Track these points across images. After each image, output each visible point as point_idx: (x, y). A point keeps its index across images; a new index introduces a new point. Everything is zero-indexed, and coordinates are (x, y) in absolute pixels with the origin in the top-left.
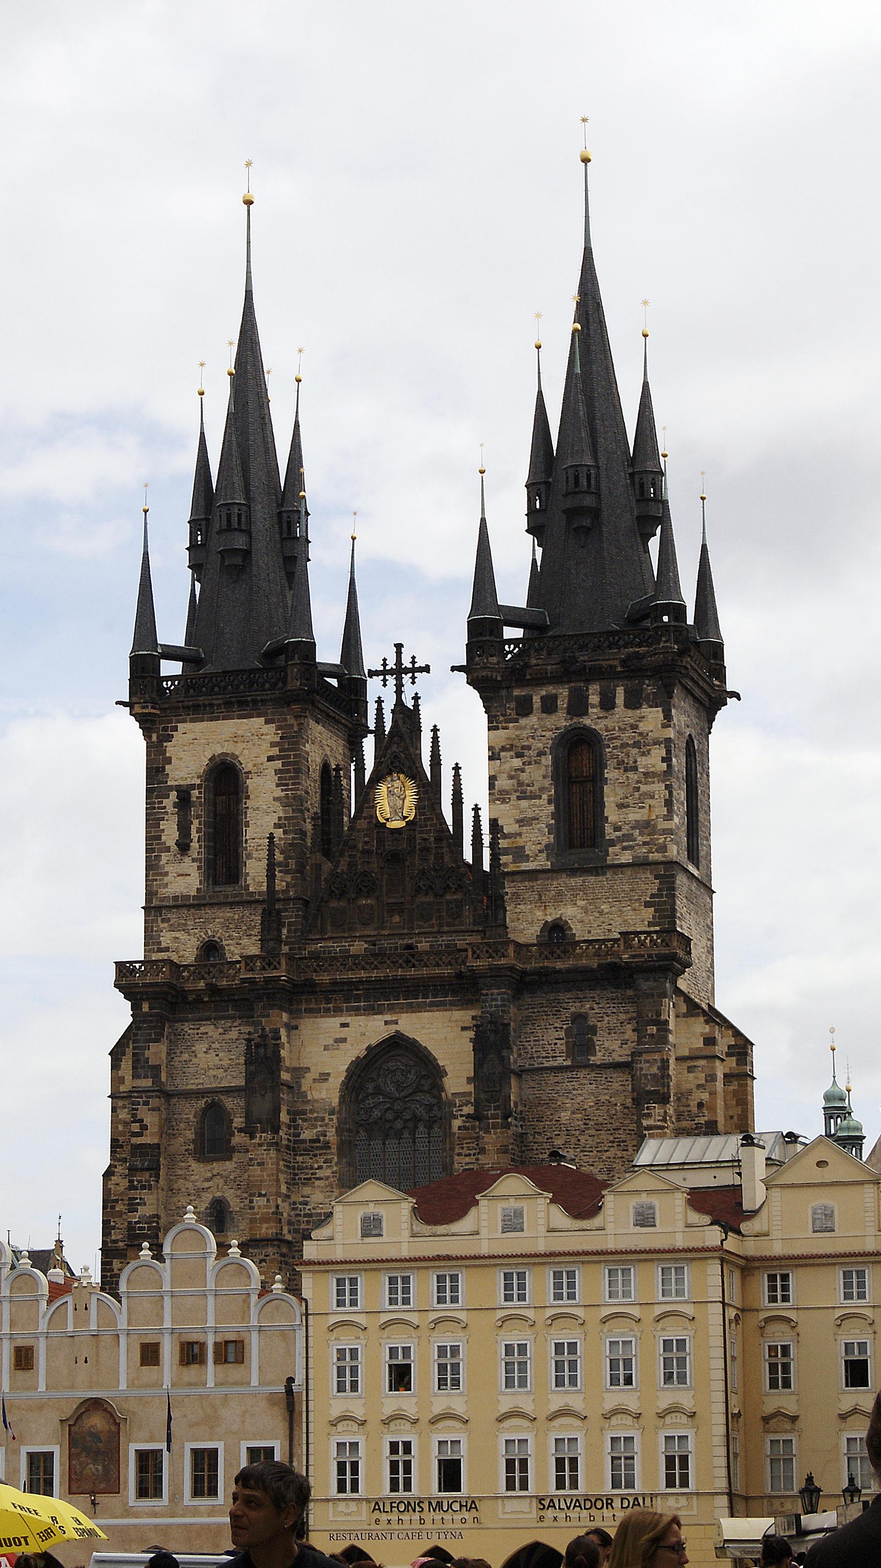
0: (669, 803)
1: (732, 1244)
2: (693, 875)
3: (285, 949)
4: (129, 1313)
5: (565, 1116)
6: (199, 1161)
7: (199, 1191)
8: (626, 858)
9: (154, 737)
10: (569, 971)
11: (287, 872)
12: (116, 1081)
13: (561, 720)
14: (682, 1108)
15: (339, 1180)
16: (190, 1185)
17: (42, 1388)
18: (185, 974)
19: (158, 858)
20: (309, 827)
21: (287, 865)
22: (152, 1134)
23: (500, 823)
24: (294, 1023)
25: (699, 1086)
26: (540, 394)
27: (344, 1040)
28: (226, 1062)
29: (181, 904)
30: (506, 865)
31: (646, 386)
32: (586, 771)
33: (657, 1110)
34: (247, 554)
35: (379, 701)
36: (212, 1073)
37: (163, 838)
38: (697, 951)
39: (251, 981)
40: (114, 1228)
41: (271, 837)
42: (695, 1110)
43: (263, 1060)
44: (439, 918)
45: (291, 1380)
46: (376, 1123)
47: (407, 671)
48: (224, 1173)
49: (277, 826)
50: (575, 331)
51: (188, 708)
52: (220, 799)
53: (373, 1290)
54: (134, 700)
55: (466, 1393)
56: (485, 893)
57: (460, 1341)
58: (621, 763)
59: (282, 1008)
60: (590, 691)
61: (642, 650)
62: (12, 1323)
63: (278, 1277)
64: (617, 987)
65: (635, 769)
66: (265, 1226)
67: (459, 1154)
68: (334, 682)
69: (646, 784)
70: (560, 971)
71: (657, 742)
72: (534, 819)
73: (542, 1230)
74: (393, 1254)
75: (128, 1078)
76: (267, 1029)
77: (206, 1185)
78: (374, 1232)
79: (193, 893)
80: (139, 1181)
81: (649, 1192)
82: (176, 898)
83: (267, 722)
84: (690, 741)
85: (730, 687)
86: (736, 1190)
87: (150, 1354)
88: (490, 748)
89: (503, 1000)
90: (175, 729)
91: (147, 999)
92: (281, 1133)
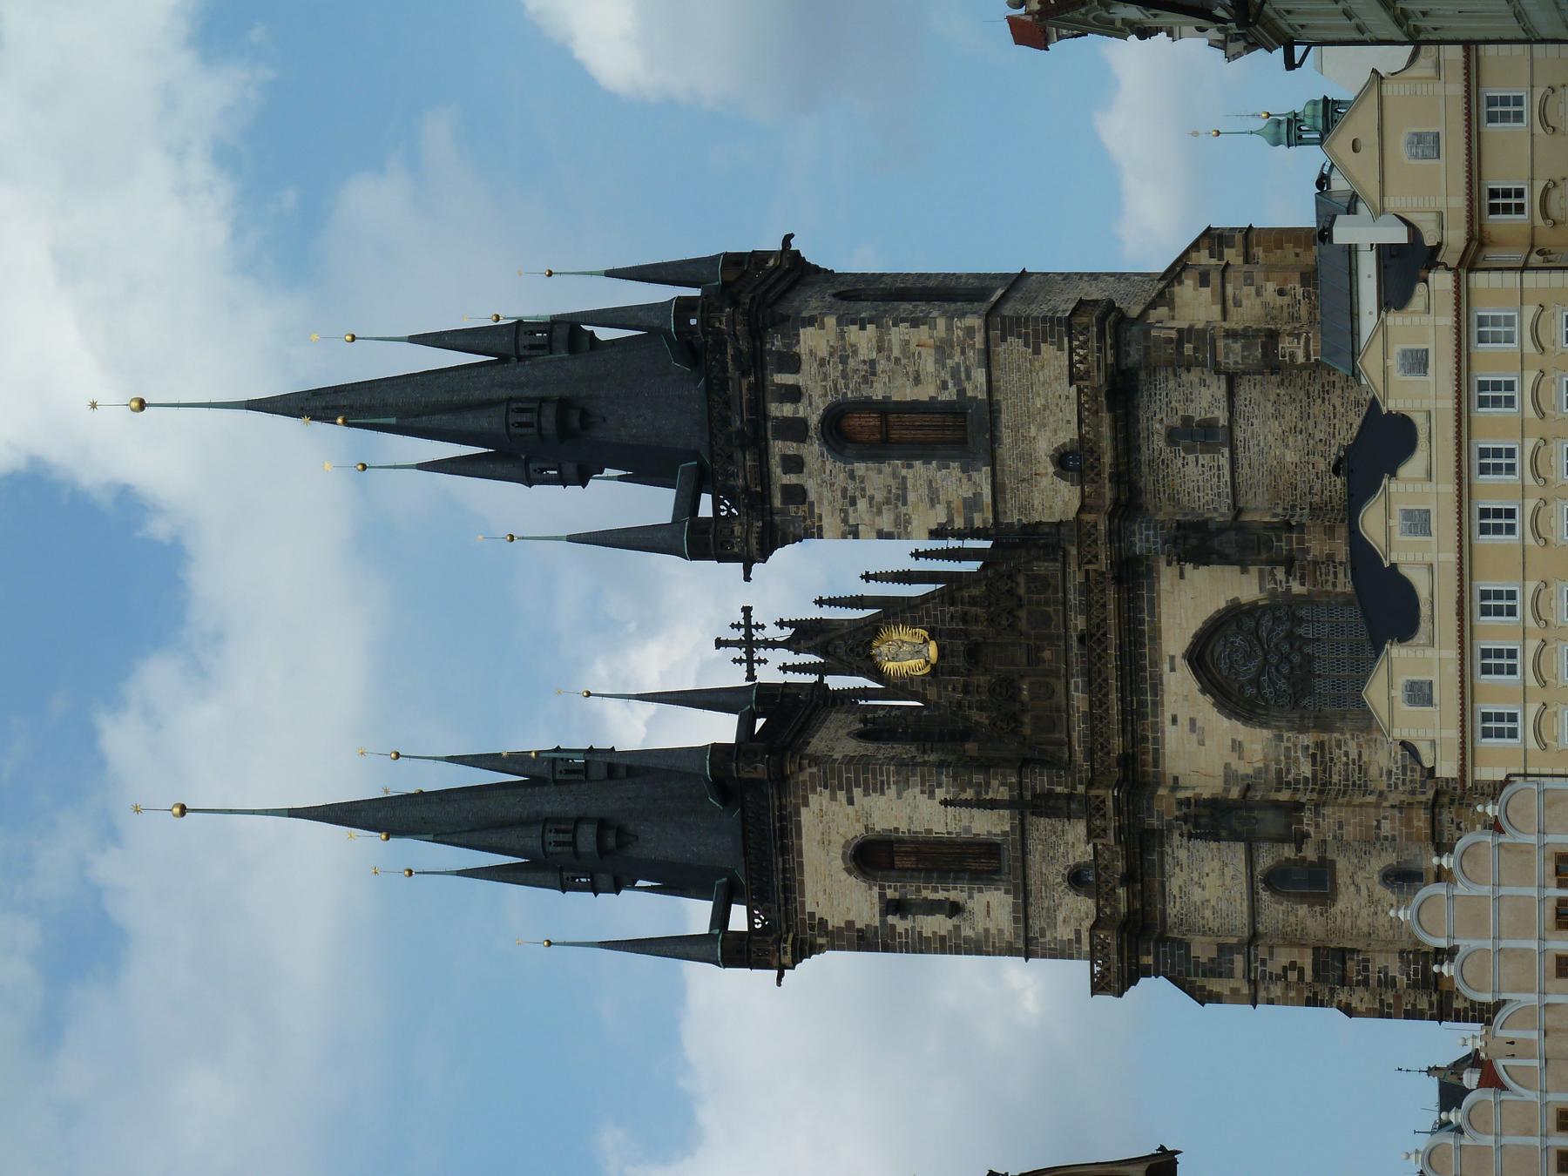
0: (915, 323)
1: (1450, 256)
2: (1003, 296)
3: (1081, 789)
5: (1290, 457)
6: (1334, 901)
7: (1372, 901)
8: (980, 375)
9: (821, 941)
10: (1115, 448)
11: (988, 785)
12: (1235, 997)
13: (812, 451)
14: (1285, 315)
16: (1364, 912)
18: (1108, 911)
19: (967, 940)
20: (933, 757)
21: (979, 785)
23: (934, 527)
24: (1170, 782)
25: (1258, 294)
26: (423, 467)
27: (1193, 722)
28: (1216, 864)
29: (1023, 914)
30: (984, 521)
31: (414, 339)
32: (873, 421)
33: (1286, 344)
34: (603, 825)
35: (785, 668)
36: (1228, 881)
37: (943, 933)
38: (1094, 293)
39: (1119, 830)
40: (1414, 1006)
41: (945, 803)
42: (1287, 300)
43: (1215, 818)
44: (1047, 603)
47: (749, 635)
48: (1351, 869)
49: (932, 795)
50: (346, 423)
51: (786, 899)
52: (898, 862)
54: (775, 962)
56: (1018, 545)
58: (865, 380)
59: (1154, 792)
61: (730, 351)
63: (1479, 808)
64: (1135, 390)
65: (873, 363)
66: (1416, 823)
67: (1334, 585)
68: (760, 722)
69: (891, 350)
70: (1116, 458)
71: (842, 336)
73: (1428, 487)
74: (1453, 669)
75: (1233, 983)
77: (1364, 892)
79: (1010, 899)
80: (1359, 973)
82: (1016, 920)
83: (806, 804)
84: (842, 296)
85: (778, 247)
86: (1385, 253)
88: (844, 536)
89: (1148, 529)
90: (812, 915)
92: (1303, 800)
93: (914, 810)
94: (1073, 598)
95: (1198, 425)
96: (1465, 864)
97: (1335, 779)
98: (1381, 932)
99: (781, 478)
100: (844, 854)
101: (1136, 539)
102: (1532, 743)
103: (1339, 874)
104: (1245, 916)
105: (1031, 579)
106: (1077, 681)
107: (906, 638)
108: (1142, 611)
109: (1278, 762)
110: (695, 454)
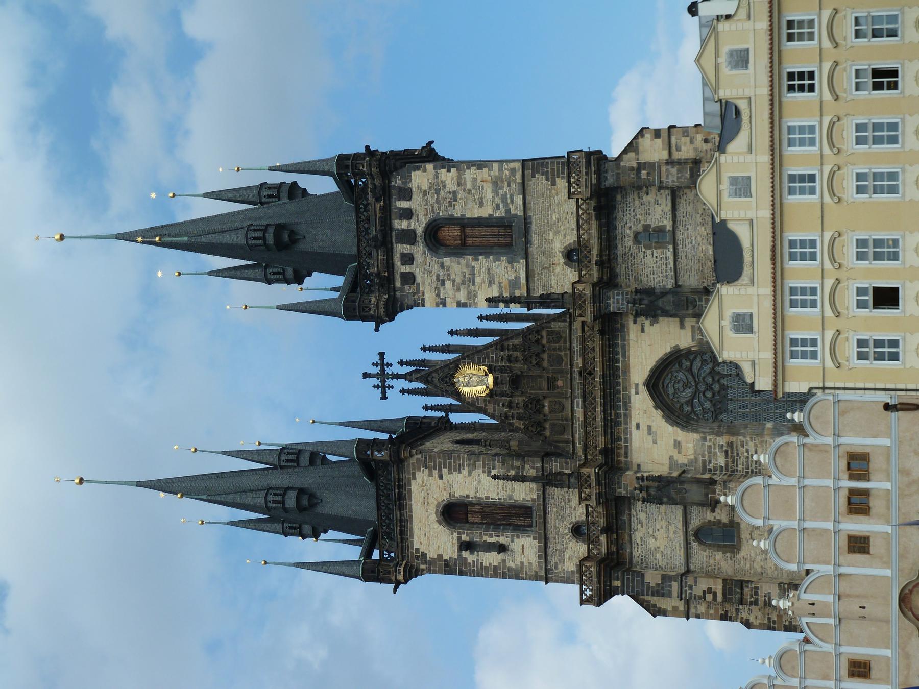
4: (819, 563)
6: (739, 550)
8: (519, 200)
9: (423, 567)
11: (523, 467)
12: (675, 613)
13: (419, 250)
15: (757, 435)
16: (759, 558)
17: (888, 653)
19: (510, 569)
22: (715, 585)
24: (635, 468)
25: (692, 142)
27: (649, 427)
28: (664, 523)
29: (544, 554)
32: (455, 231)
34: (301, 491)
36: (671, 535)
39: (599, 496)
40: (790, 622)
42: (709, 145)
43: (662, 489)
44: (560, 349)
45: (887, 407)
46: (714, 405)
53: (802, 323)
54: (393, 578)
55: (902, 233)
57: (852, 238)
58: (450, 204)
60: (399, 227)
62: (826, 677)
63: (789, 415)
64: (614, 208)
65: (455, 193)
70: (601, 251)
71: (436, 176)
72: (489, 273)
73: (750, 158)
74: (768, 304)
76: (637, 486)
78: (748, 321)
79: (536, 543)
80: (751, 596)
81: (717, 55)
82: (540, 557)
83: (415, 479)
87: (859, 545)
88: (437, 305)
89: (618, 294)
90: (417, 550)
91: (610, 582)
93: (477, 483)
94: (576, 346)
95: (654, 230)
96: (778, 459)
97: (740, 467)
98: (769, 572)
99: (401, 268)
100: (437, 511)
101: (611, 301)
102: (829, 363)
103: (742, 532)
104: (682, 558)
105: (550, 333)
106: (578, 401)
107: (474, 372)
108: (617, 354)
109: (703, 456)
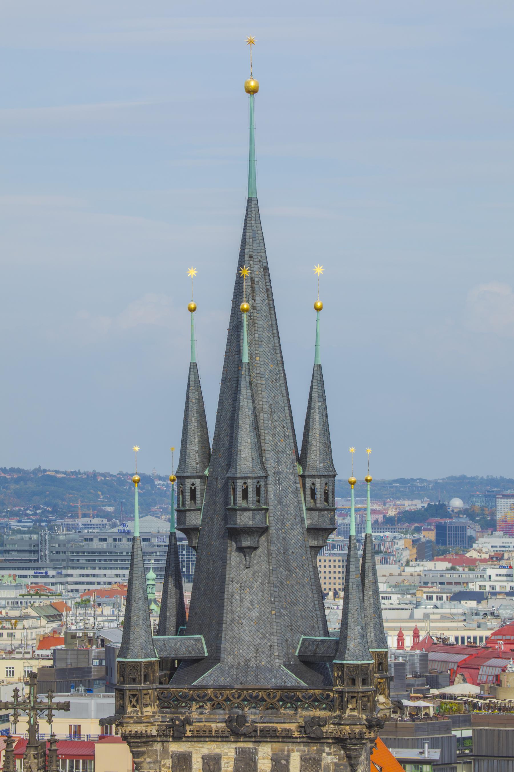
60: (260, 754)
110: (215, 658)
